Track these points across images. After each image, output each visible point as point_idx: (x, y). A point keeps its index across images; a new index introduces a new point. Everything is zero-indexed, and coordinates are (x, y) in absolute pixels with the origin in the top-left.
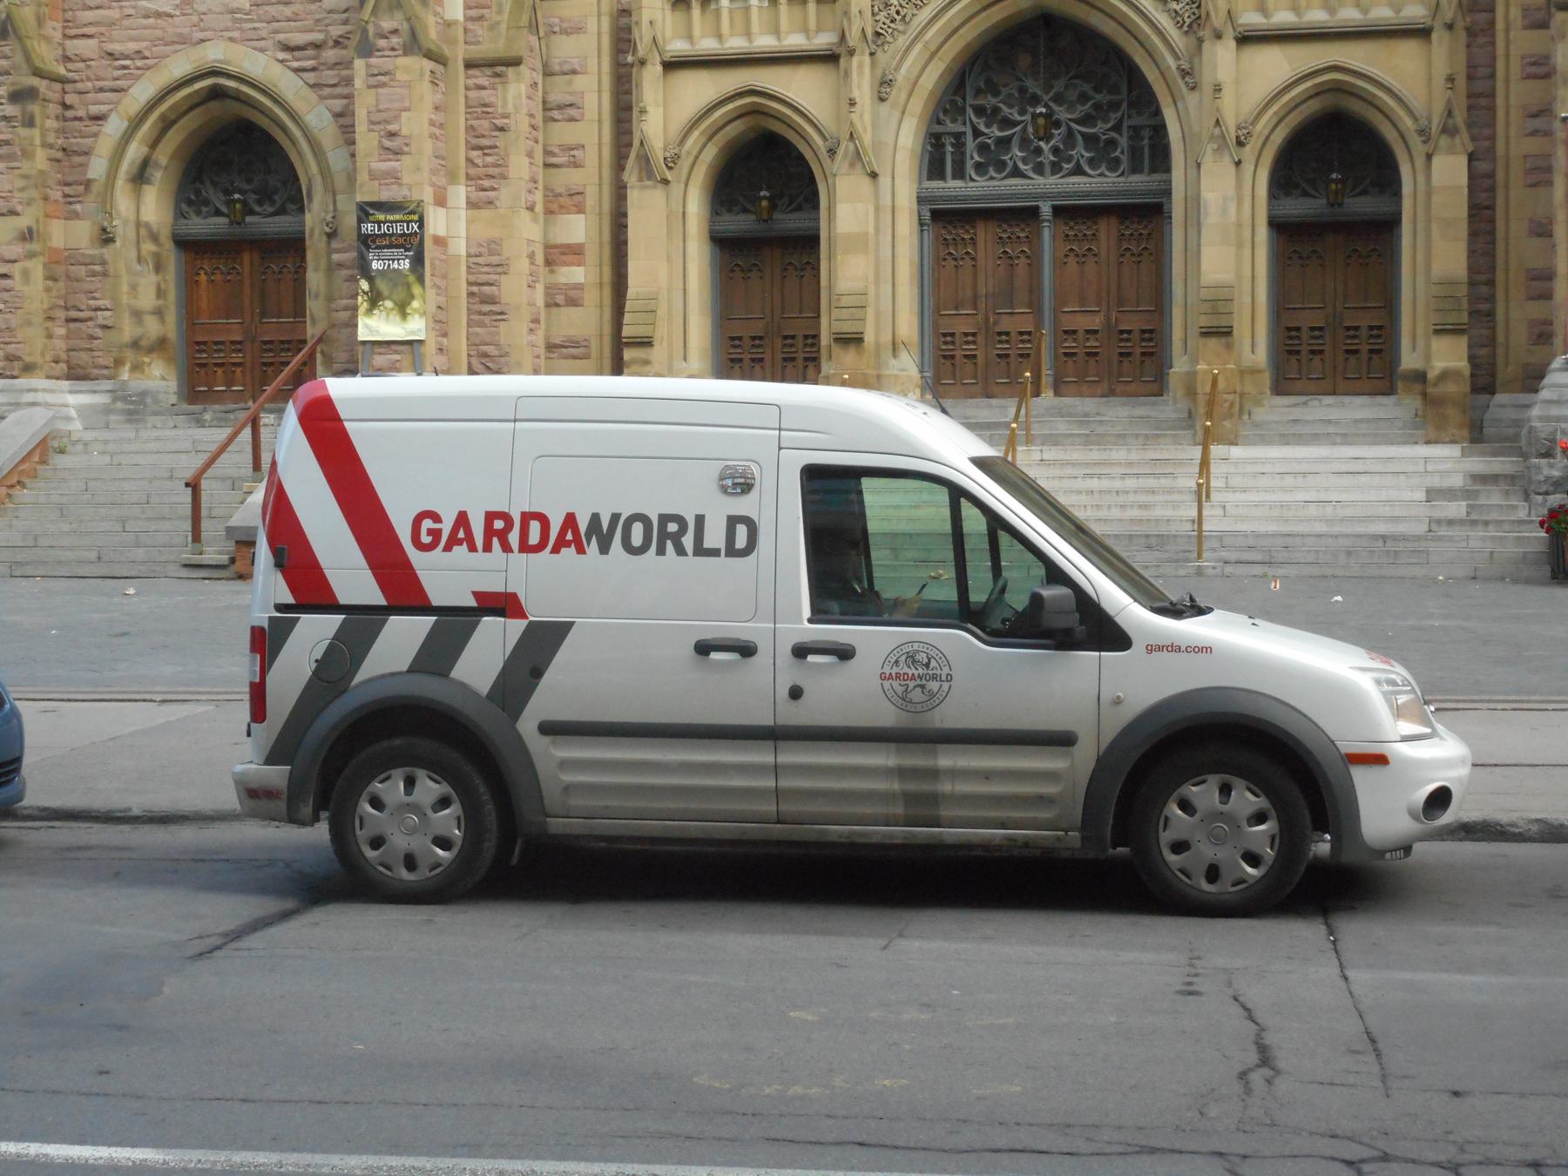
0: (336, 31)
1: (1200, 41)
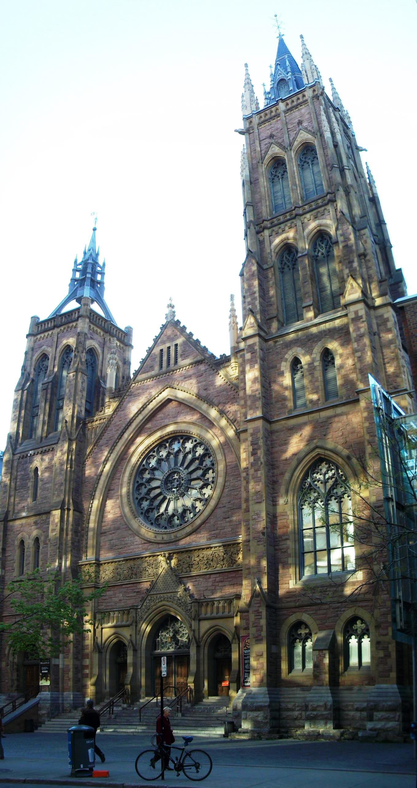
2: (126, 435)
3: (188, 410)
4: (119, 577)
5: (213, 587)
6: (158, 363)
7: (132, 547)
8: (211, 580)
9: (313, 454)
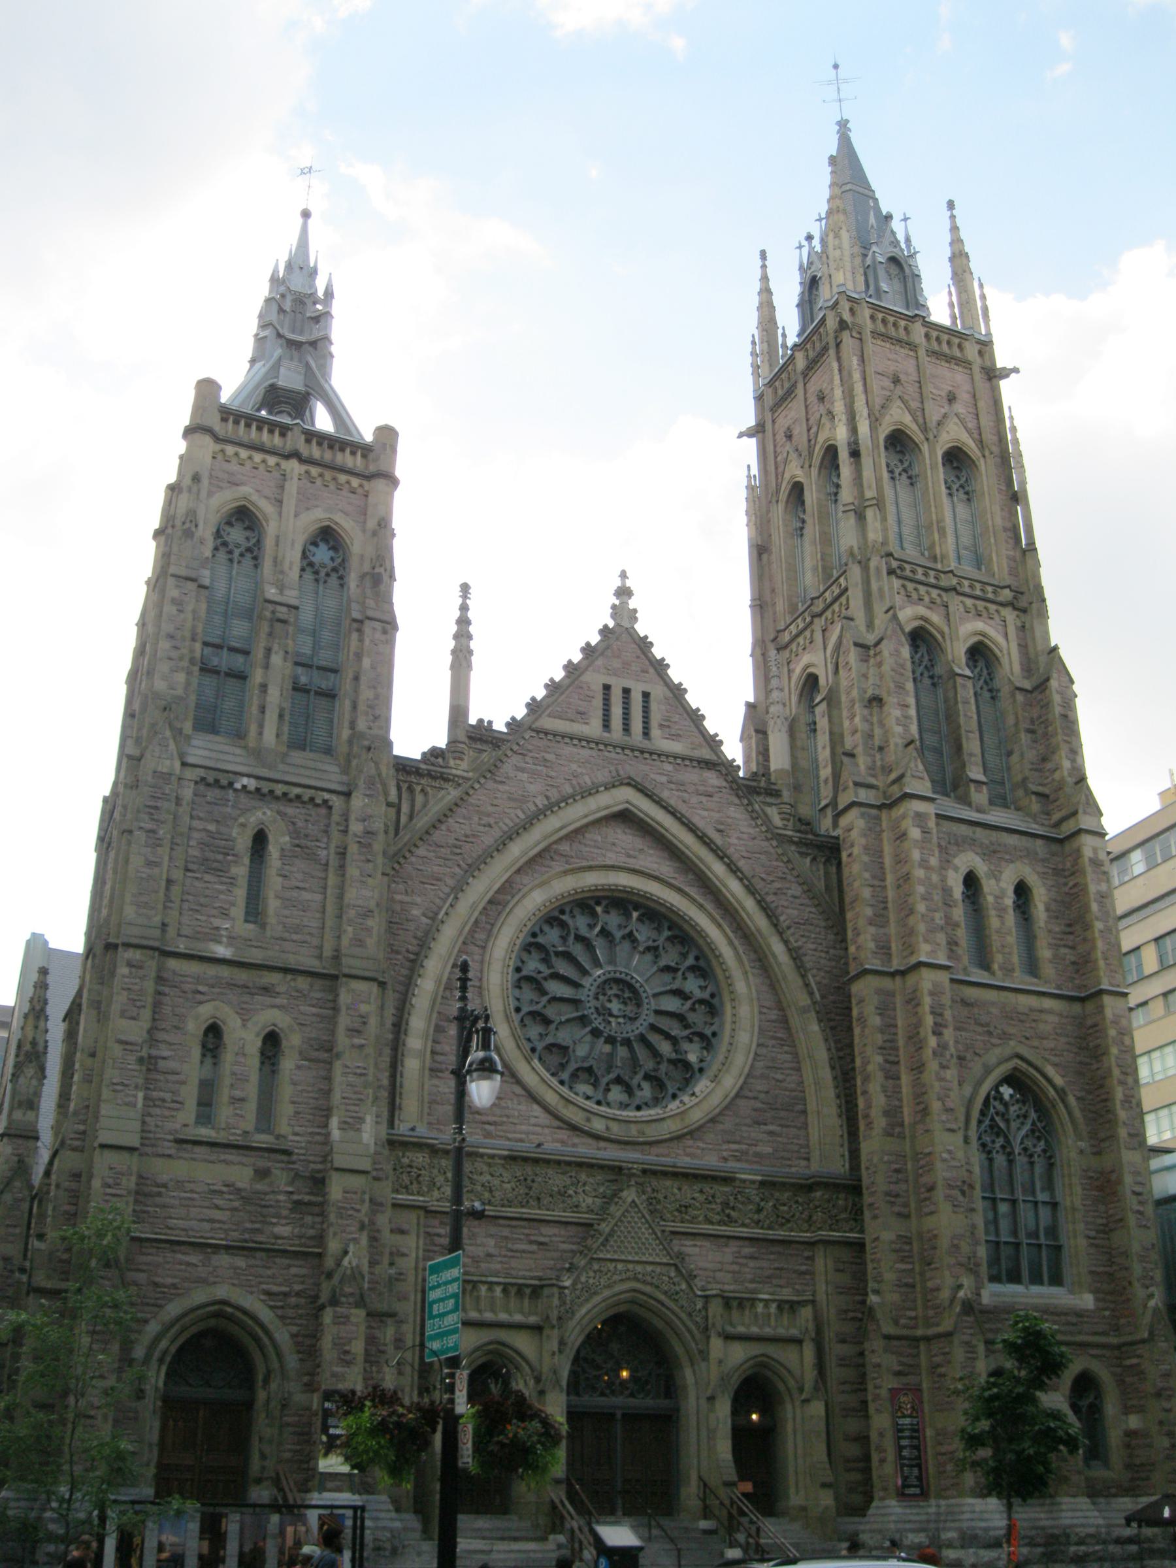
0: (297, 1287)
1: (708, 1337)
2: (517, 850)
4: (487, 1195)
5: (736, 1268)
6: (600, 713)
7: (524, 1128)
9: (1009, 1065)
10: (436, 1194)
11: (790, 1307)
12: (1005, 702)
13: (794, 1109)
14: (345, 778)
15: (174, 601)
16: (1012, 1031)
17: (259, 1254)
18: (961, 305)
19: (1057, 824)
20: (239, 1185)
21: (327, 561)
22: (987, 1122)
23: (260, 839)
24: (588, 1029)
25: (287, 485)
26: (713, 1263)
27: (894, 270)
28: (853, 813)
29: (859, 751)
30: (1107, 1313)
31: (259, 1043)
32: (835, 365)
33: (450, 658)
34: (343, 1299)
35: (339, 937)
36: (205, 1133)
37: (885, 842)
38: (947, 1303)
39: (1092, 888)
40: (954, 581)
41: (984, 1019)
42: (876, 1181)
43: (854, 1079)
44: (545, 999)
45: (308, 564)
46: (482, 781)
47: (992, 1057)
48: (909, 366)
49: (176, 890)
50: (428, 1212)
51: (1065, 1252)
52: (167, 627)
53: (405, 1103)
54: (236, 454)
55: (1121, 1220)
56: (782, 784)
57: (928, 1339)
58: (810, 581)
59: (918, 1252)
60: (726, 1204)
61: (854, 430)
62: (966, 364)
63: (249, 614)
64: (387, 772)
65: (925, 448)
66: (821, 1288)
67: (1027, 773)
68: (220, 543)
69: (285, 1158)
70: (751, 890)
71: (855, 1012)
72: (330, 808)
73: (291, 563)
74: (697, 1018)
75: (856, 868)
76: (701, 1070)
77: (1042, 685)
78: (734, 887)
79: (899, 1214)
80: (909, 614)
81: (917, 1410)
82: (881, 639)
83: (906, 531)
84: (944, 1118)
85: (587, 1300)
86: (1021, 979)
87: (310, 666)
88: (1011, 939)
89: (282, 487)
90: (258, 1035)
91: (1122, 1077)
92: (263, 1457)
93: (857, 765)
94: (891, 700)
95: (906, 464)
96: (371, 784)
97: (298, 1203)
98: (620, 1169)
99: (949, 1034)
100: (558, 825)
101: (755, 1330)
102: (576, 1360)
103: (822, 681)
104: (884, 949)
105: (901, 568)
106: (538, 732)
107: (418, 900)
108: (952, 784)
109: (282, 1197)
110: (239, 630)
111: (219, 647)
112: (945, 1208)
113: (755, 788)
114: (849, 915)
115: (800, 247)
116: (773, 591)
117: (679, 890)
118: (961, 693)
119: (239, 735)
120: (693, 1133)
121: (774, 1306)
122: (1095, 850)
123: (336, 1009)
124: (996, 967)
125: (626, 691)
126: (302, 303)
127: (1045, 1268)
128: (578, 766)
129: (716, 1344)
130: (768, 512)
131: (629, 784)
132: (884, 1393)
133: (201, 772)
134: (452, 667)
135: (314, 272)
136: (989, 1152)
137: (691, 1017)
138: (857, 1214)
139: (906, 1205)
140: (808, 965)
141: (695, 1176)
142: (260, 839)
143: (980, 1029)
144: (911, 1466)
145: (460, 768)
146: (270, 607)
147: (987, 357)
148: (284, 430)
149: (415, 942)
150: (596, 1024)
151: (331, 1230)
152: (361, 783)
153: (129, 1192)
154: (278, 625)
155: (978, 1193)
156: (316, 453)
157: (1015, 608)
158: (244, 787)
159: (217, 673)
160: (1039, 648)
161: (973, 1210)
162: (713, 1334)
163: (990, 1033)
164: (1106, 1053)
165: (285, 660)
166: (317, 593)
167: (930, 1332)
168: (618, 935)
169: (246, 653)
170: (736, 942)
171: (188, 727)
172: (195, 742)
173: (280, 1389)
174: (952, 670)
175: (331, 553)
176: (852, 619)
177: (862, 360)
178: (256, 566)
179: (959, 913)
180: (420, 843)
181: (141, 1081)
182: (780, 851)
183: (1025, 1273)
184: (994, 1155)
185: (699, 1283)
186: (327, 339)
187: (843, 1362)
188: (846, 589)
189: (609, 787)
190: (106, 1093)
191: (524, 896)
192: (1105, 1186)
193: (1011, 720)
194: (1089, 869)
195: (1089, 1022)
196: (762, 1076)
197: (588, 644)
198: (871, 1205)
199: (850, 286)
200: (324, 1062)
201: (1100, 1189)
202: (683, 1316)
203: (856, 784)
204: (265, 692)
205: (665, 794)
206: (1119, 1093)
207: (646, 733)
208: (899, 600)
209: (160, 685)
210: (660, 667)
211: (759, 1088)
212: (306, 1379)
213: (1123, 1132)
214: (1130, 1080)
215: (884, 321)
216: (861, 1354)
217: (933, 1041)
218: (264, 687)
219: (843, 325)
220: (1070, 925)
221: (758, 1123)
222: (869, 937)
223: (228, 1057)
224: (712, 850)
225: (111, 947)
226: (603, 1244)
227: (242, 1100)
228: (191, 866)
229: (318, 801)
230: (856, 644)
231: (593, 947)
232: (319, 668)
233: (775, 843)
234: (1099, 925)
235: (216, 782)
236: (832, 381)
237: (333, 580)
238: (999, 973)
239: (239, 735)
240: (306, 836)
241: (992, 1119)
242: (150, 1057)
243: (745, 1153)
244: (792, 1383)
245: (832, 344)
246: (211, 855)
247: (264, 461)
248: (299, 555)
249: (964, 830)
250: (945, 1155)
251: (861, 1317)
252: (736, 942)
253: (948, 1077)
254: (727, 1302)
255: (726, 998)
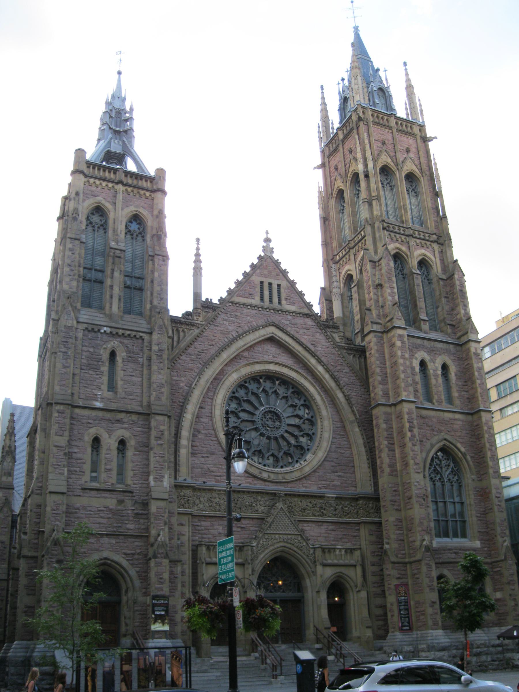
0: (138, 551)
1: (316, 565)
2: (225, 356)
3: (290, 356)
4: (218, 507)
5: (326, 535)
6: (259, 294)
8: (322, 527)
9: (441, 444)
10: (196, 507)
11: (350, 551)
12: (435, 285)
13: (348, 465)
14: (149, 326)
15: (70, 249)
16: (443, 428)
17: (121, 537)
18: (411, 109)
19: (459, 338)
20: (111, 507)
21: (137, 230)
22: (433, 469)
23: (113, 354)
24: (259, 433)
25: (118, 195)
26: (317, 534)
27: (381, 94)
28: (371, 335)
29: (373, 308)
30: (486, 549)
31: (117, 444)
32: (357, 137)
33: (192, 271)
34: (159, 555)
35: (150, 397)
36: (95, 485)
37: (385, 348)
38: (418, 547)
39: (475, 365)
40: (412, 232)
41: (430, 423)
42: (386, 496)
43: (375, 451)
44: (240, 420)
45: (128, 231)
46: (209, 325)
47: (434, 440)
48: (389, 137)
49: (77, 378)
50: (193, 516)
51: (467, 524)
52: (68, 261)
53: (181, 469)
54: (94, 182)
55: (491, 509)
56: (339, 323)
57: (411, 563)
58: (347, 232)
59: (406, 526)
60: (321, 508)
61: (366, 166)
62: (413, 135)
63: (103, 254)
64: (167, 323)
65: (397, 173)
66: (363, 543)
67: (445, 316)
68: (89, 223)
69: (130, 495)
70: (327, 370)
71: (374, 422)
72: (143, 339)
73: (121, 231)
74: (306, 427)
75: (373, 359)
76: (308, 450)
77: (451, 277)
78: (320, 369)
79: (397, 510)
80: (392, 247)
81: (407, 594)
82: (381, 259)
83: (390, 210)
84: (415, 467)
85: (263, 551)
86: (445, 406)
87: (131, 277)
88: (441, 389)
89: (115, 197)
90: (116, 441)
91: (490, 447)
92: (127, 625)
93: (372, 314)
94: (386, 285)
95: (389, 180)
96: (161, 328)
97: (137, 514)
98: (275, 494)
99: (416, 431)
100: (243, 344)
101: (335, 562)
102: (259, 577)
103: (354, 277)
104: (386, 395)
105: (389, 227)
106: (232, 303)
107: (183, 379)
108: (413, 321)
109: (130, 512)
110: (99, 261)
111: (91, 269)
112: (416, 506)
113: (327, 325)
114: (371, 380)
115: (339, 84)
116: (331, 238)
117: (296, 371)
118: (416, 281)
119: (101, 308)
120: (306, 477)
121: (343, 551)
122: (476, 349)
123: (149, 428)
124: (435, 401)
125: (270, 284)
126: (120, 113)
127: (459, 530)
128: (251, 318)
129: (320, 569)
130: (328, 202)
131: (273, 325)
132: (392, 587)
133: (85, 325)
134: (194, 275)
135: (124, 100)
136: (434, 481)
137: (303, 427)
138: (378, 510)
139: (399, 506)
140: (353, 402)
141: (308, 496)
142: (113, 354)
143: (428, 428)
144: (405, 618)
145: (199, 320)
146: (113, 251)
147: (423, 132)
148: (115, 171)
149: (182, 397)
150: (262, 431)
151: (152, 526)
152: (156, 328)
153: (63, 512)
154: (117, 259)
155: (430, 499)
156: (130, 181)
157: (438, 243)
158: (105, 331)
159: (90, 281)
160: (449, 261)
161: (428, 507)
162: (318, 563)
163: (433, 430)
164: (483, 437)
165: (120, 274)
166: (133, 244)
167: (412, 560)
168: (270, 392)
169: (102, 271)
170: (322, 393)
171: (79, 305)
172: (82, 312)
173: (132, 596)
174: (411, 271)
175: (138, 226)
176: (368, 250)
177: (369, 134)
178: (105, 233)
179: (418, 378)
180: (182, 354)
181: (66, 463)
182: (339, 353)
183: (451, 534)
184: (436, 482)
185: (311, 542)
186: (131, 129)
187: (374, 574)
188: (365, 236)
189: (264, 327)
190: (50, 469)
191: (229, 376)
192: (484, 494)
193: (438, 293)
194: (473, 357)
195: (475, 424)
196: (335, 452)
197: (253, 264)
198: (384, 506)
199: (362, 101)
200: (145, 451)
201: (482, 496)
202: (305, 556)
203: (372, 323)
204: (112, 289)
205: (289, 329)
206: (489, 454)
207: (280, 303)
208: (388, 241)
209: (65, 287)
210: (284, 273)
211: (334, 457)
212: (144, 590)
213: (491, 471)
214: (493, 448)
215: (377, 117)
216: (382, 570)
217: (409, 434)
218: (111, 287)
219: (360, 119)
220: (465, 382)
221: (334, 472)
222: (380, 390)
223: (103, 452)
224: (310, 353)
225: (49, 404)
226: (269, 527)
227: (110, 470)
228: (83, 367)
229: (138, 337)
230: (370, 261)
231: (260, 397)
232: (135, 277)
233: (337, 349)
234: (478, 382)
235: (92, 329)
236: (355, 144)
237: (140, 238)
238: (436, 404)
239: (101, 308)
240: (133, 352)
241: (435, 467)
242: (69, 452)
243: (329, 485)
244: (352, 584)
245: (355, 127)
246: (92, 362)
247: (107, 185)
248: (124, 227)
249: (419, 341)
250: (416, 484)
251: (381, 554)
252: (322, 393)
253: (416, 450)
254: (323, 550)
255: (318, 417)
